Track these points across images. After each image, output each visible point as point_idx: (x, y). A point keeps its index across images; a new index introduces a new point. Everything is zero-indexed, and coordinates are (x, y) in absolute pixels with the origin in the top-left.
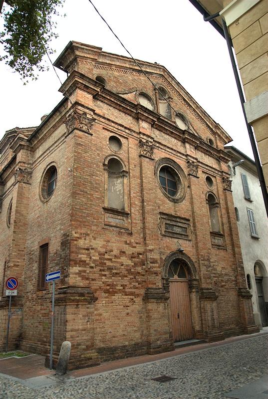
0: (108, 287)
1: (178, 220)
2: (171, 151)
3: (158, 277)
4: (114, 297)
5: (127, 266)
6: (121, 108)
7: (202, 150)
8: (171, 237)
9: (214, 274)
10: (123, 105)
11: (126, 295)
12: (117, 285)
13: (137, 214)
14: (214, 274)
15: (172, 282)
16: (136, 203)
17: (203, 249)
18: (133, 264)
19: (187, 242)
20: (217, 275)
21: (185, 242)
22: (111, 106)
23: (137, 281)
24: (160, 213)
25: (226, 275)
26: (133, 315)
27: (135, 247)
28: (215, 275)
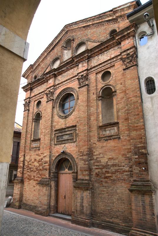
0: (29, 177)
1: (66, 130)
2: (67, 82)
3: (47, 171)
4: (30, 182)
5: (36, 166)
6: (40, 84)
7: (96, 54)
8: (60, 144)
9: (96, 166)
10: (40, 82)
11: (35, 181)
12: (32, 176)
14: (96, 166)
15: (62, 174)
17: (83, 146)
18: (39, 165)
19: (72, 144)
20: (100, 167)
21: (70, 144)
22: (37, 87)
23: (40, 174)
25: (113, 165)
26: (36, 191)
27: (40, 156)
28: (97, 167)
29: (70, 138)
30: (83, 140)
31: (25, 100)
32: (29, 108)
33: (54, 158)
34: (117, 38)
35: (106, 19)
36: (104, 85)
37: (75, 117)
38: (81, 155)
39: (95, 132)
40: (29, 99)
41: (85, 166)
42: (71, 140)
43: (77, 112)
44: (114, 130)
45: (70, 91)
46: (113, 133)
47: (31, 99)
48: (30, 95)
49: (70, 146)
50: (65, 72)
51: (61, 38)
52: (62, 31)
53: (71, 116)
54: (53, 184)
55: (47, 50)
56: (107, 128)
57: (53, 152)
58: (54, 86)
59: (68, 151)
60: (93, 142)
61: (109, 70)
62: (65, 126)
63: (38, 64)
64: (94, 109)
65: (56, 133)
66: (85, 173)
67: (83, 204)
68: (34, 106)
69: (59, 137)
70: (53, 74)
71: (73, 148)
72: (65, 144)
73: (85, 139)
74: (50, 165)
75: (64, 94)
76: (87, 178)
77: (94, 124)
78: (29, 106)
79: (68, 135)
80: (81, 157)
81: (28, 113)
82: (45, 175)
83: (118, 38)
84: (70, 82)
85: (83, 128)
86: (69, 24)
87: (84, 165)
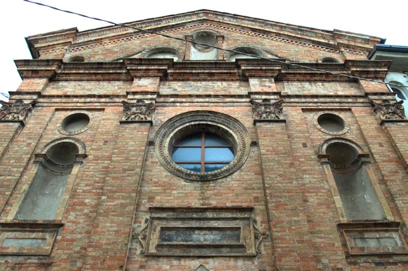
1: (210, 215)
6: (99, 77)
7: (298, 77)
8: (179, 258)
10: (100, 72)
13: (81, 221)
16: (87, 201)
19: (240, 263)
21: (232, 262)
22: (81, 80)
24: (150, 208)
29: (225, 242)
30: (295, 254)
31: (11, 93)
32: (25, 119)
34: (355, 69)
35: (312, 39)
36: (330, 137)
37: (245, 185)
39: (331, 236)
40: (35, 97)
43: (252, 174)
44: (390, 240)
45: (218, 123)
46: (390, 248)
47: (41, 100)
48: (44, 89)
50: (199, 80)
51: (186, 23)
52: (193, 15)
53: (229, 179)
55: (138, 24)
56: (367, 231)
60: (332, 265)
62: (203, 204)
63: (96, 38)
64: (314, 178)
65: (159, 219)
68: (49, 121)
69: (173, 233)
70: (159, 70)
72: (202, 260)
73: (303, 251)
75: (193, 123)
77: (322, 215)
78: (27, 115)
79: (214, 232)
81: (16, 132)
83: (357, 71)
84: (217, 102)
85: (287, 219)
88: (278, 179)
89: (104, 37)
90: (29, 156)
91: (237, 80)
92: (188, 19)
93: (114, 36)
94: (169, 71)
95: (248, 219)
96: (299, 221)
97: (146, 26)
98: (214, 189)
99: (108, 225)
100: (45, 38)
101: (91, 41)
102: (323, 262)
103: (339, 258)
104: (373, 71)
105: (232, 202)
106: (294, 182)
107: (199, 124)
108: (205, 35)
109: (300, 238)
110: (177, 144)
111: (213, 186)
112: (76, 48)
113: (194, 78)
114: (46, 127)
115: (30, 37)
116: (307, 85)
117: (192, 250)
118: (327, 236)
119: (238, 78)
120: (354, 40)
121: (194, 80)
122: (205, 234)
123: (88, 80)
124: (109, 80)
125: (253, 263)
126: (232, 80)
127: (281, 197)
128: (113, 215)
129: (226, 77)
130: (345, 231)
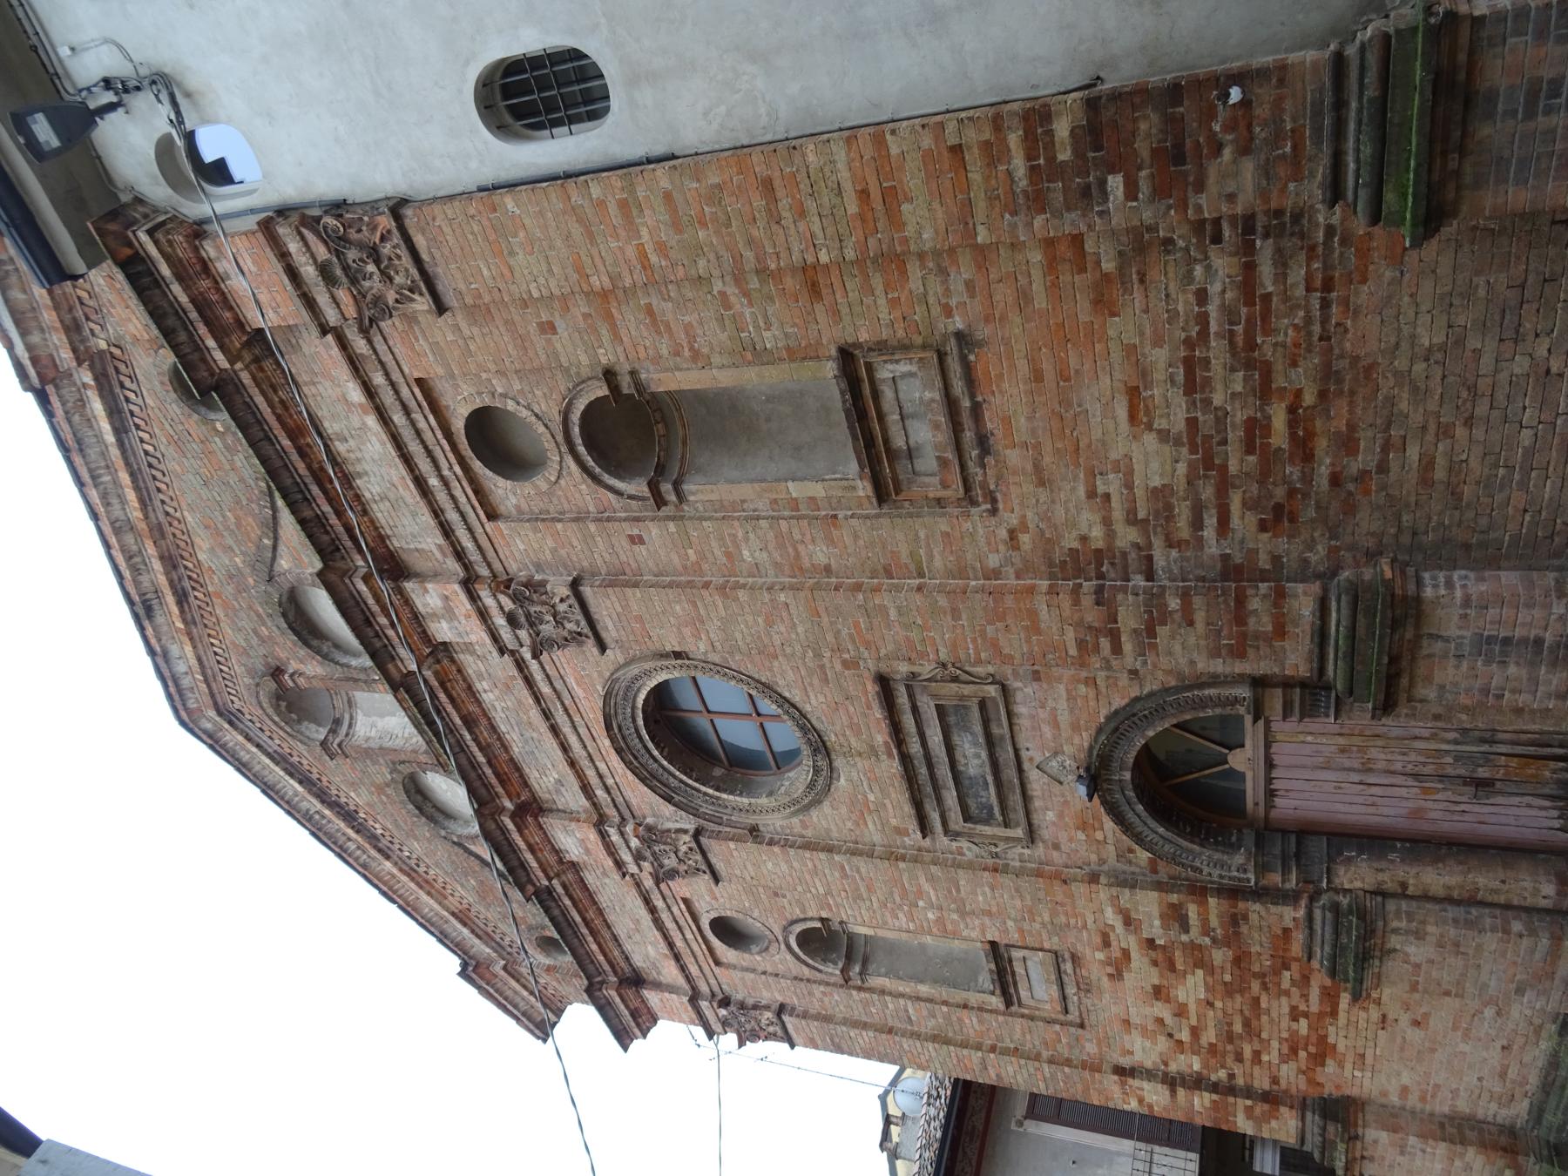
0: (1302, 1054)
1: (915, 747)
2: (566, 729)
3: (1253, 917)
4: (1341, 1048)
5: (1208, 988)
6: (591, 914)
8: (1026, 798)
9: (1197, 524)
10: (578, 919)
11: (1334, 1013)
12: (1294, 1034)
14: (1197, 524)
17: (1038, 631)
18: (1200, 973)
19: (1021, 709)
20: (1208, 492)
21: (1024, 723)
22: (615, 938)
23: (1277, 973)
25: (1194, 381)
26: (1423, 1010)
27: (1126, 954)
28: (1211, 521)
29: (978, 728)
30: (990, 629)
31: (710, 1034)
32: (767, 1007)
33: (1143, 856)
34: (219, 356)
35: (110, 438)
36: (570, 461)
37: (816, 681)
38: (1105, 643)
39: (922, 535)
40: (704, 1004)
41: (1200, 617)
42: (992, 716)
43: (776, 664)
44: (902, 386)
45: (634, 708)
46: (928, 395)
47: (704, 988)
48: (671, 989)
49: (1036, 727)
50: (499, 739)
51: (269, 755)
52: (223, 746)
53: (807, 708)
54: (1357, 875)
55: (356, 859)
56: (886, 441)
57: (1094, 857)
58: (600, 823)
59: (1077, 744)
60: (1002, 548)
61: (459, 425)
62: (890, 755)
63: (459, 926)
64: (747, 540)
65: (944, 823)
66: (1261, 619)
67: (1549, 637)
68: (754, 971)
70: (520, 830)
71: (1050, 703)
72: (1026, 766)
74: (1199, 891)
75: (656, 753)
76: (1303, 602)
77: (861, 542)
78: (755, 1007)
79: (956, 739)
80: (1128, 647)
81: (805, 1015)
82: (1286, 931)
83: (222, 347)
84: (566, 710)
86: (170, 697)
87: (1191, 623)
88: (783, 629)
89: (446, 914)
90: (854, 993)
91: (453, 661)
92: (248, 752)
93: (429, 894)
94: (508, 805)
95: (908, 687)
96: (899, 609)
97: (349, 839)
98: (844, 735)
99: (981, 898)
100: (524, 1014)
101: (473, 931)
102: (998, 564)
103: (981, 531)
104: (186, 289)
105: (869, 707)
106: (783, 599)
107: (652, 739)
108: (283, 704)
109: (945, 613)
110: (721, 761)
111: (836, 735)
112: (509, 949)
113: (498, 751)
114: (771, 974)
115: (538, 1038)
116: (370, 487)
117: (1004, 777)
118: (923, 543)
119: (445, 662)
120: (30, 315)
121: (506, 748)
122: (965, 756)
123: (609, 928)
124: (590, 895)
125: (1018, 689)
126: (459, 671)
127: (839, 632)
128: (958, 891)
129: (459, 689)
130: (897, 494)
